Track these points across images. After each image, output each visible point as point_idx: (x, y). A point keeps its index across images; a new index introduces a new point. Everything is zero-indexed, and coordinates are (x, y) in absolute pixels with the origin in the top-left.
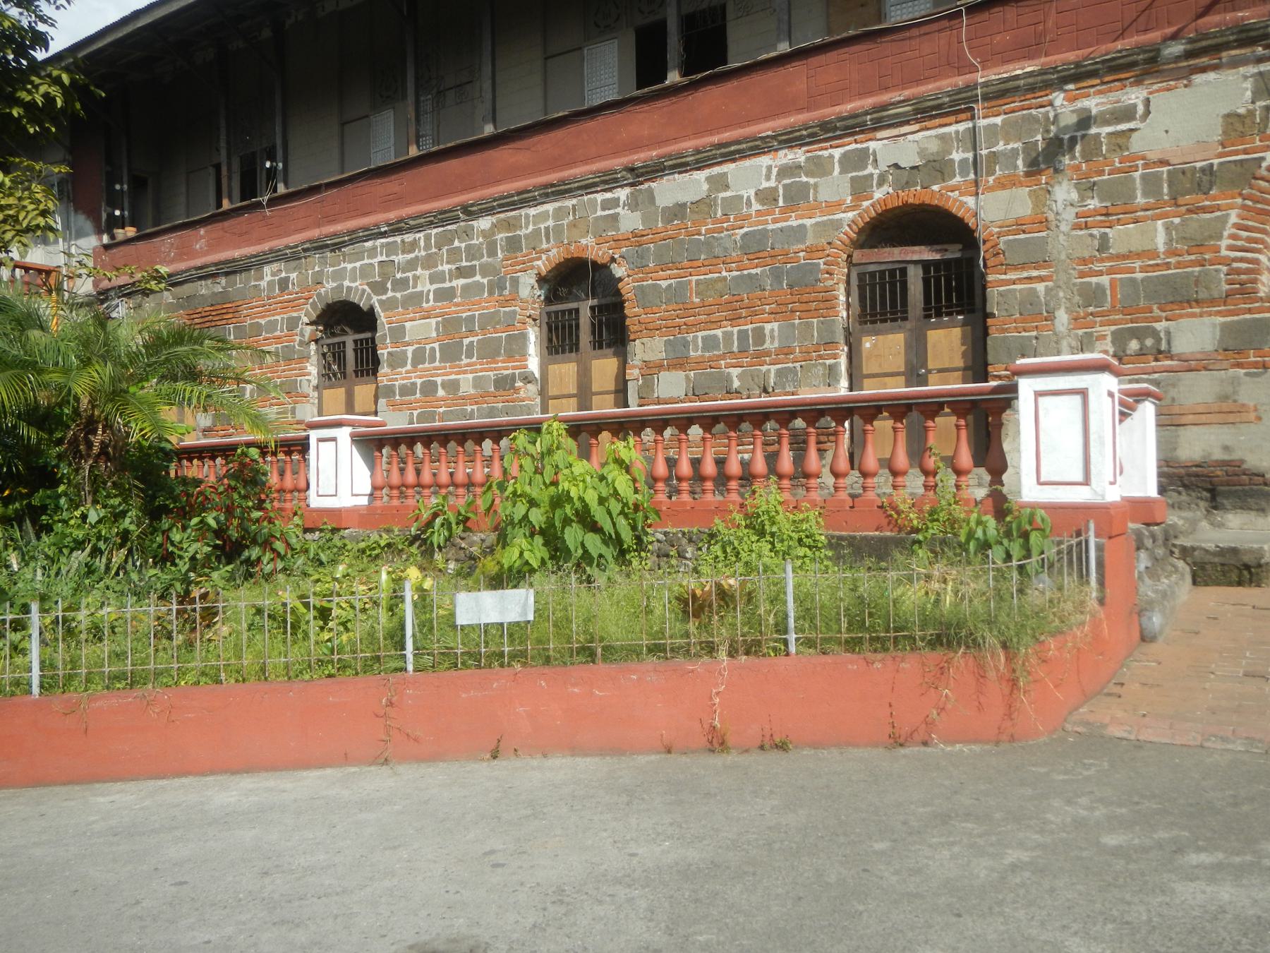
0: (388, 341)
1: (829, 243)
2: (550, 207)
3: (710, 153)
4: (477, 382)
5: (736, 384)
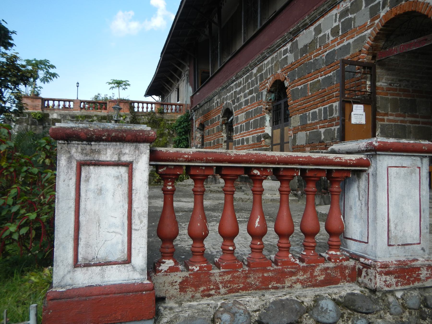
1: (360, 51)
2: (269, 59)
5: (323, 137)
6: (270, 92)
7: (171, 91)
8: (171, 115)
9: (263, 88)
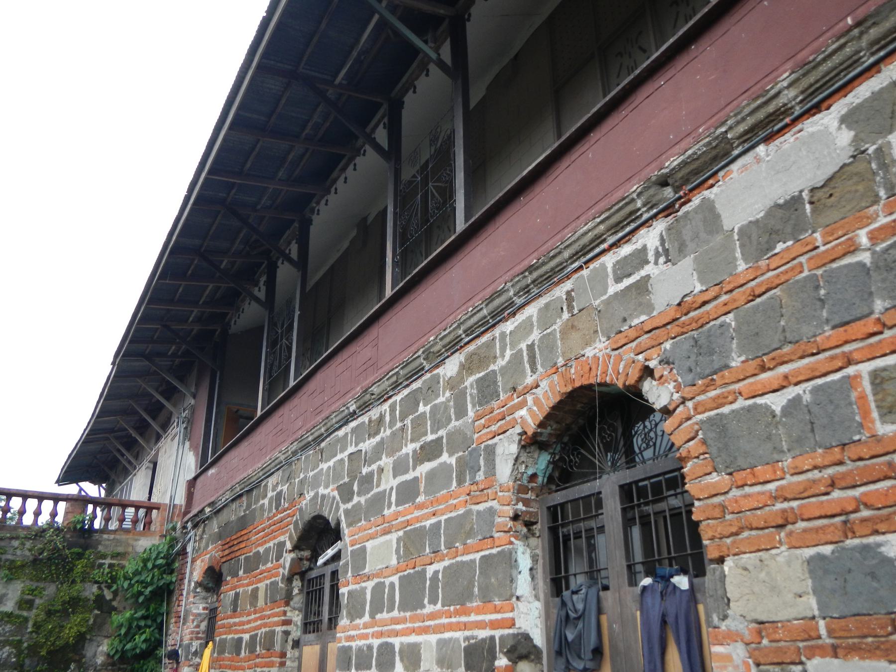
0: (350, 574)
2: (532, 311)
3: (837, 59)
7: (135, 468)
8: (118, 537)
9: (494, 428)
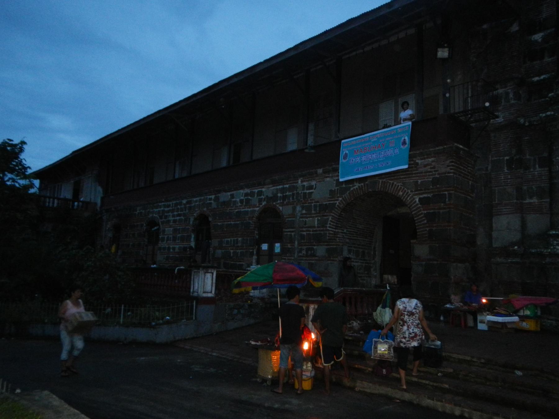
2: (198, 199)
4: (179, 248)
5: (232, 255)
6: (195, 219)
